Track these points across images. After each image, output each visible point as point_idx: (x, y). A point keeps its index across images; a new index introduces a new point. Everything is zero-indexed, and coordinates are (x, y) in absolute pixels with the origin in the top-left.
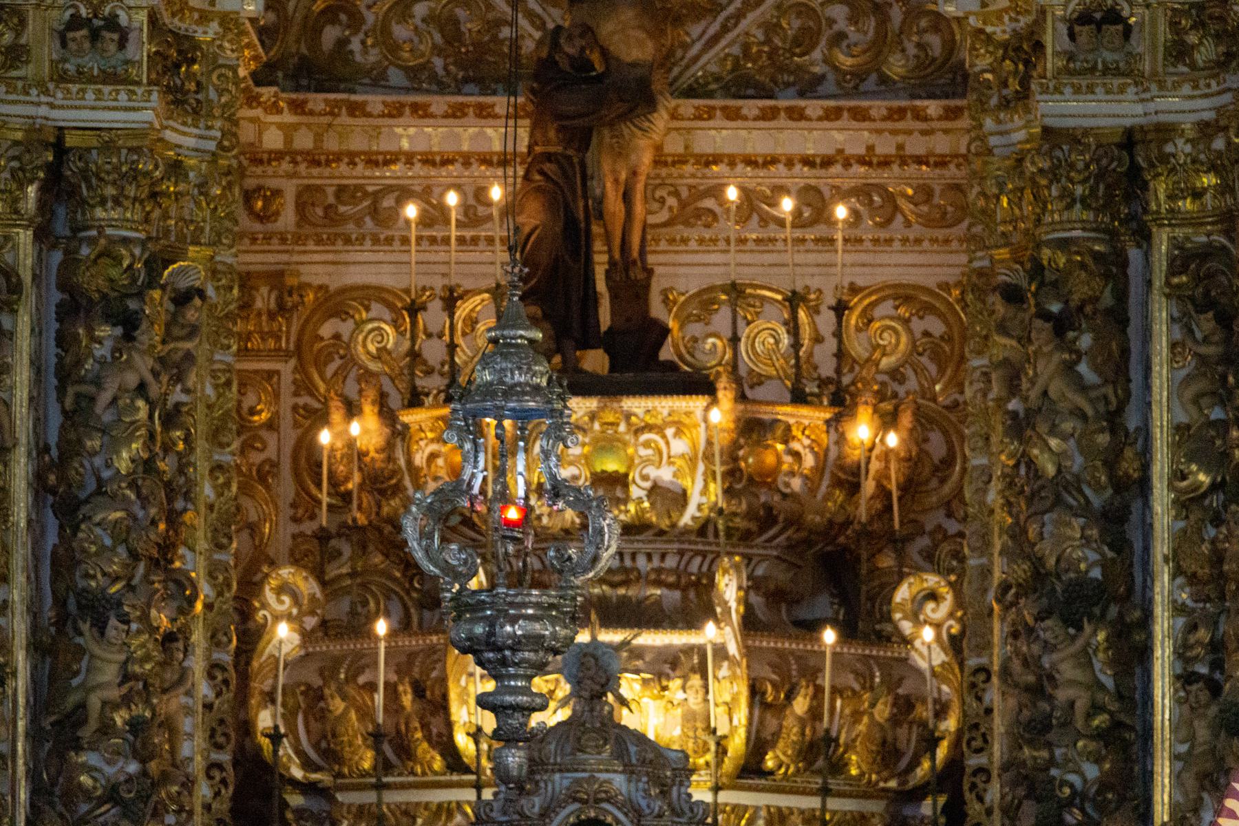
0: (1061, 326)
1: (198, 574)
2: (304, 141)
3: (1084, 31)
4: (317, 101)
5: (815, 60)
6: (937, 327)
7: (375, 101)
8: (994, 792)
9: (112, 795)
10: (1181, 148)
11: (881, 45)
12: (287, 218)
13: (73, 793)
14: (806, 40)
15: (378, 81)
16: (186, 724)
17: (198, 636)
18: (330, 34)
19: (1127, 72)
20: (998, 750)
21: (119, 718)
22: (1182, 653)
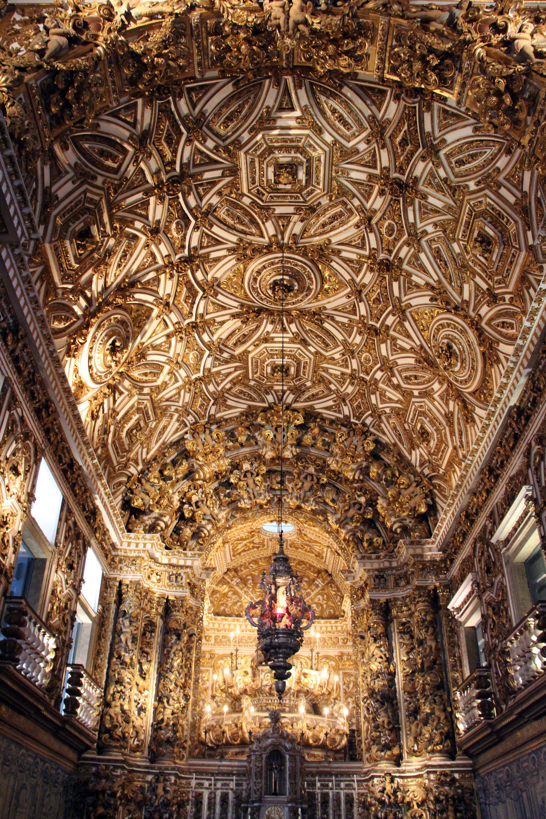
1: (191, 693)
2: (216, 626)
3: (377, 581)
4: (219, 618)
6: (333, 663)
7: (230, 619)
8: (363, 746)
9: (168, 741)
11: (322, 611)
12: (213, 640)
15: (230, 615)
16: (186, 727)
17: (190, 708)
18: (222, 608)
19: (385, 588)
20: (364, 735)
21: (171, 723)
22: (408, 710)
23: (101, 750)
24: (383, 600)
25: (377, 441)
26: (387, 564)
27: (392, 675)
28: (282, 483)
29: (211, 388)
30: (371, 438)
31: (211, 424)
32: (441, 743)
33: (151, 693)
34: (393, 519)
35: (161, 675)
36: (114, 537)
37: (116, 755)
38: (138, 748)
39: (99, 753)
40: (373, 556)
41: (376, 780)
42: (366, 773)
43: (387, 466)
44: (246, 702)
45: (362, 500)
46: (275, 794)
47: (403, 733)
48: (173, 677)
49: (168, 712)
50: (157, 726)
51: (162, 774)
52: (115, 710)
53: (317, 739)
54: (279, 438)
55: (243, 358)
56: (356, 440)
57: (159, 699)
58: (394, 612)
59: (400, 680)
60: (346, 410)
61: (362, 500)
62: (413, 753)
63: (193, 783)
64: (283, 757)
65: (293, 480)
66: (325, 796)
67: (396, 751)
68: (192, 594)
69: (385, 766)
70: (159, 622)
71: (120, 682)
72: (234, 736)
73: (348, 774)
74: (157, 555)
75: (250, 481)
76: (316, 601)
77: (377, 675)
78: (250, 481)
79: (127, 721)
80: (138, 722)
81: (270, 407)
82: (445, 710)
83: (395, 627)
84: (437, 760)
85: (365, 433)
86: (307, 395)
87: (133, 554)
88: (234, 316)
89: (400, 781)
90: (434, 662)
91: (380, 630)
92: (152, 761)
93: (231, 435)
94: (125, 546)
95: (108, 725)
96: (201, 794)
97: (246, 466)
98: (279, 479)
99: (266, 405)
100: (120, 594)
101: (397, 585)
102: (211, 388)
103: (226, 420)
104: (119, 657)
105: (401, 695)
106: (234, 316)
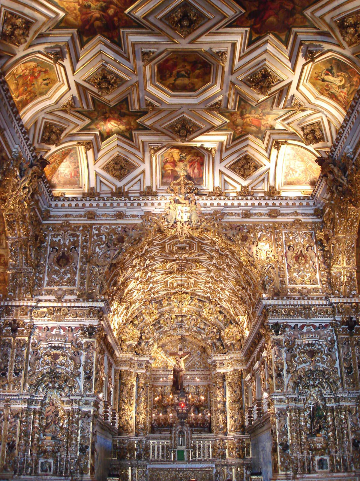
0: (219, 389)
5: (195, 367)
9: (142, 429)
10: (228, 374)
11: (200, 365)
13: (139, 429)
14: (194, 365)
20: (214, 424)
23: (120, 434)
24: (222, 373)
25: (221, 307)
26: (224, 358)
27: (225, 402)
28: (182, 321)
29: (153, 291)
30: (219, 306)
31: (152, 300)
32: (240, 429)
33: (134, 411)
34: (226, 341)
35: (138, 404)
36: (117, 355)
37: (124, 436)
38: (131, 432)
39: (119, 435)
40: (219, 355)
41: (217, 441)
42: (214, 438)
43: (225, 316)
44: (169, 410)
45: (215, 330)
46: (181, 446)
47: (228, 424)
48: (142, 405)
49: (141, 418)
50: (137, 424)
51: (141, 441)
52: (123, 420)
53: (197, 424)
54: (181, 306)
55: (166, 283)
56: (212, 306)
57: (137, 414)
58: (226, 378)
59: (228, 404)
60: (209, 295)
61: (215, 330)
62: (231, 431)
63: (151, 442)
64: (184, 433)
65: (186, 320)
66: (200, 446)
67: (225, 430)
68: (147, 370)
69: (221, 436)
70: (135, 383)
71: (124, 410)
72: (165, 424)
73: (208, 438)
74: (133, 358)
75: (169, 322)
76: (198, 360)
77: (220, 402)
78: (169, 322)
79: (128, 423)
80: (130, 423)
81: (177, 292)
82: (242, 417)
83: (227, 383)
84: (239, 435)
85: (216, 304)
86: (191, 289)
87: (124, 359)
88: (162, 274)
89: (226, 441)
90: (239, 399)
91: (221, 385)
92: (136, 436)
93: (161, 304)
94: (121, 356)
95: (121, 425)
96: (154, 446)
97: (167, 316)
98: (181, 319)
99: (174, 291)
100: (120, 375)
101: (228, 366)
102: (153, 291)
103: (158, 297)
104: (123, 400)
105: (228, 411)
106: (162, 274)
